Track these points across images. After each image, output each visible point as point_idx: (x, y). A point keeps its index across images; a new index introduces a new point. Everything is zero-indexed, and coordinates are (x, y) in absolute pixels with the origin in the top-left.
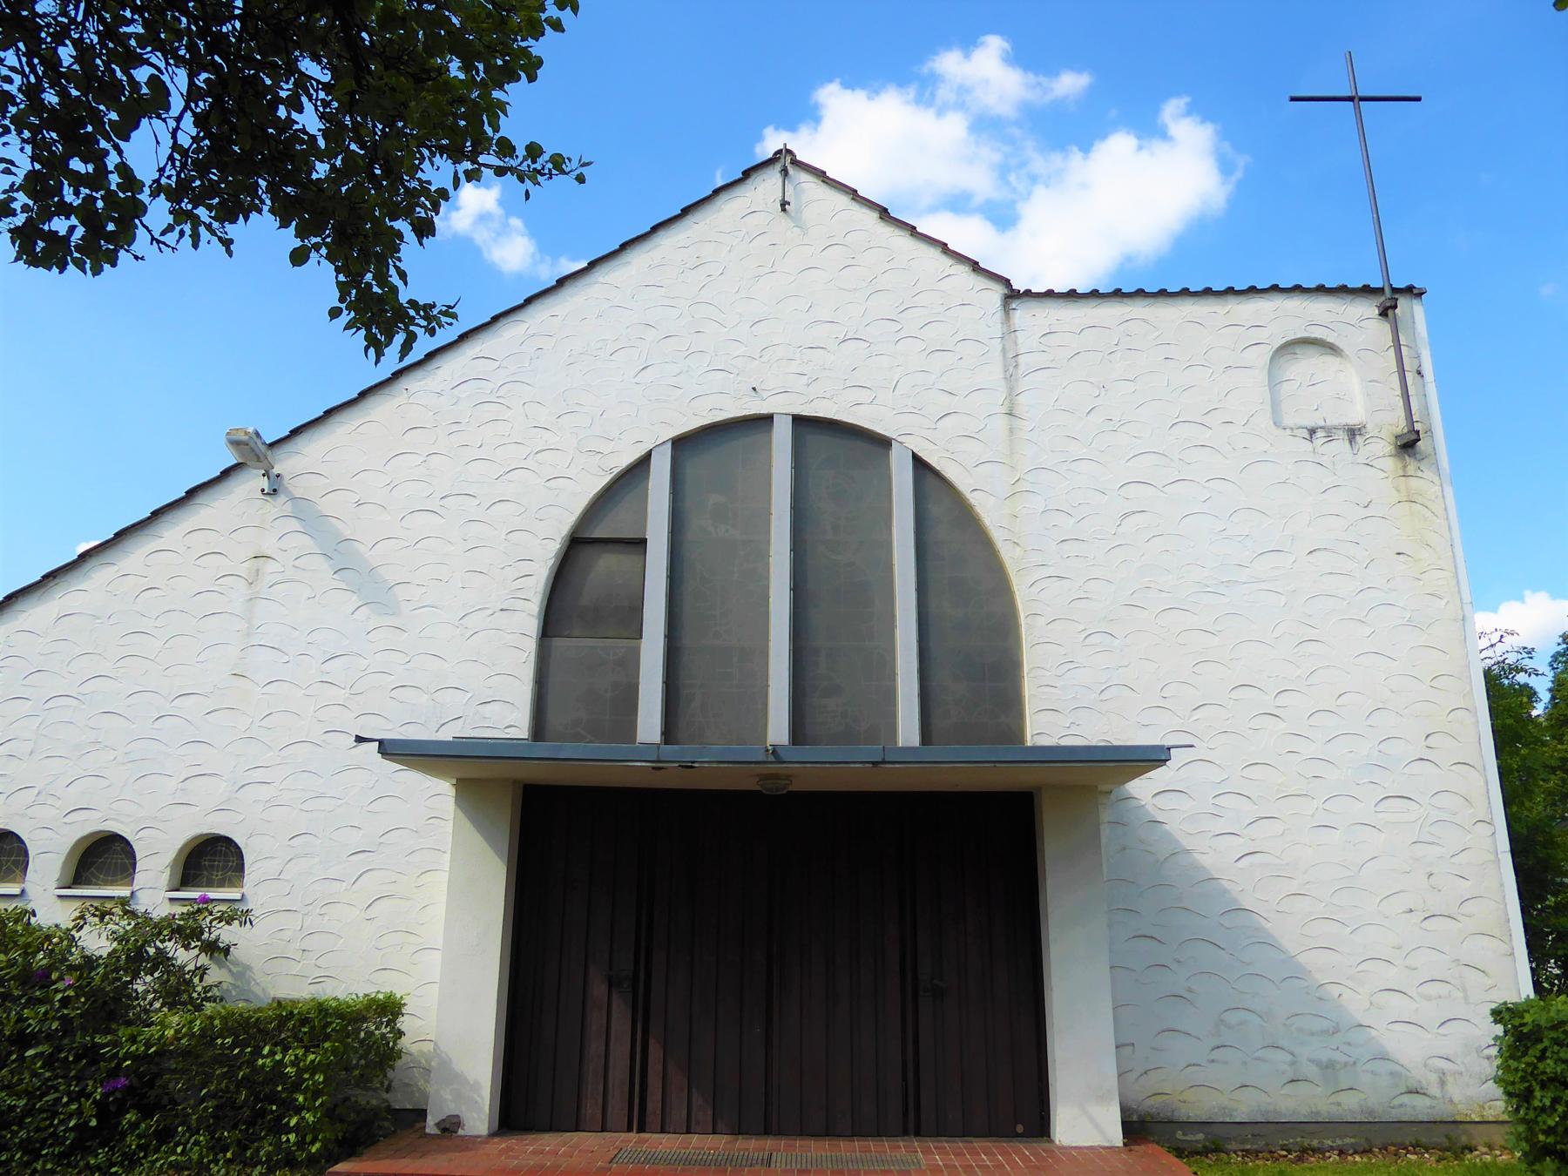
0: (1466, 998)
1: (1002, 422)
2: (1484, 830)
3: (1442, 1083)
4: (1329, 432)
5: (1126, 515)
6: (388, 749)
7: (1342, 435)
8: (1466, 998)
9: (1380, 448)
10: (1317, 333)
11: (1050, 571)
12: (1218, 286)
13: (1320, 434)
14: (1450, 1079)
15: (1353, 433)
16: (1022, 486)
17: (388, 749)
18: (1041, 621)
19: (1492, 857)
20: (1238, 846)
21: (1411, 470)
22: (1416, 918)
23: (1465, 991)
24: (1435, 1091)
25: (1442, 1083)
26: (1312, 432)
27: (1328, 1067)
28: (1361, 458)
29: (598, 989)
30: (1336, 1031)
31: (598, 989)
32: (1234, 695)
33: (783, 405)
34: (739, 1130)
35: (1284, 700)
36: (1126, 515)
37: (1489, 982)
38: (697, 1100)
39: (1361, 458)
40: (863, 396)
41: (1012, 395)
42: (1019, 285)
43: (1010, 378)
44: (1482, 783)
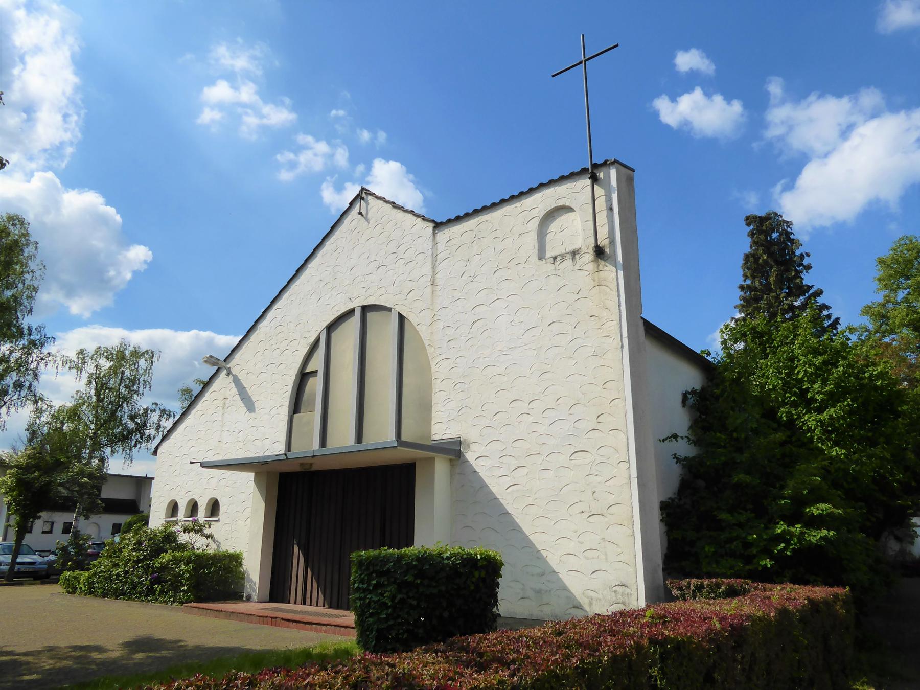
0: (606, 559)
1: (429, 290)
2: (624, 466)
3: (591, 604)
4: (563, 256)
5: (474, 323)
6: (204, 465)
7: (569, 256)
8: (606, 559)
9: (589, 255)
10: (561, 203)
11: (443, 357)
12: (525, 190)
13: (559, 258)
14: (595, 602)
15: (574, 254)
16: (435, 318)
17: (204, 465)
18: (439, 380)
19: (627, 481)
20: (508, 481)
21: (601, 267)
22: (586, 515)
23: (606, 554)
24: (587, 608)
25: (591, 604)
26: (555, 258)
27: (539, 592)
28: (577, 267)
29: (296, 548)
30: (542, 574)
31: (296, 548)
32: (511, 406)
33: (357, 303)
34: (330, 607)
35: (533, 405)
36: (474, 323)
37: (620, 551)
38: (320, 593)
39: (577, 267)
40: (383, 291)
41: (434, 274)
42: (438, 221)
43: (434, 267)
44: (625, 440)
